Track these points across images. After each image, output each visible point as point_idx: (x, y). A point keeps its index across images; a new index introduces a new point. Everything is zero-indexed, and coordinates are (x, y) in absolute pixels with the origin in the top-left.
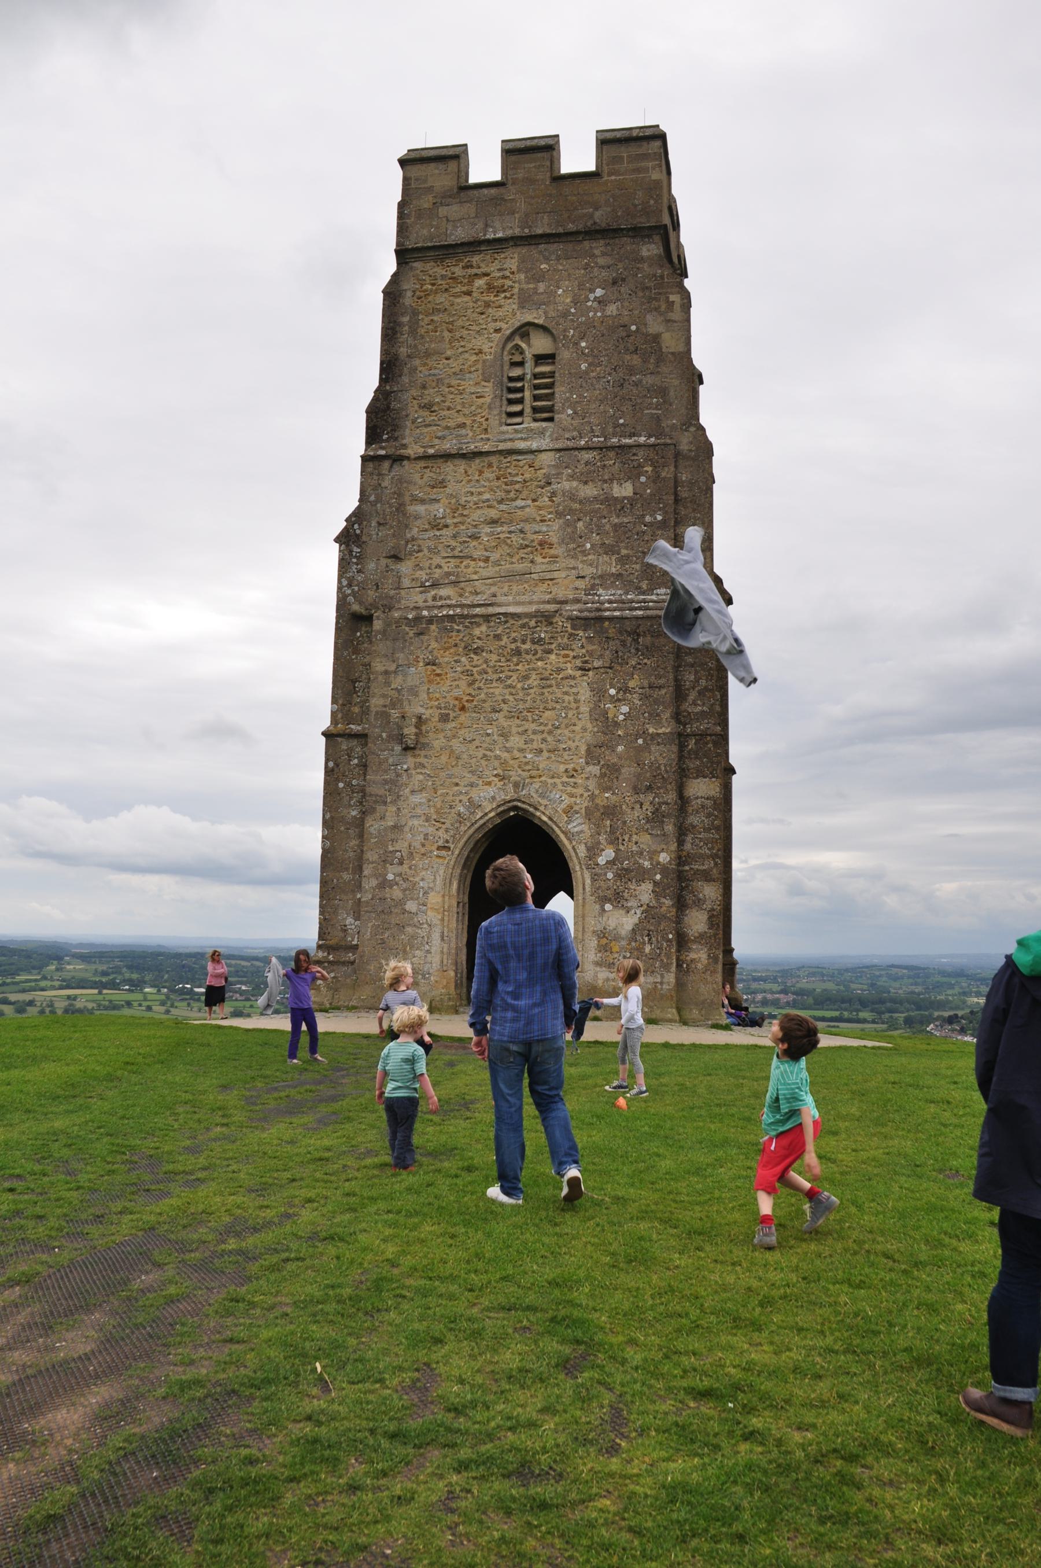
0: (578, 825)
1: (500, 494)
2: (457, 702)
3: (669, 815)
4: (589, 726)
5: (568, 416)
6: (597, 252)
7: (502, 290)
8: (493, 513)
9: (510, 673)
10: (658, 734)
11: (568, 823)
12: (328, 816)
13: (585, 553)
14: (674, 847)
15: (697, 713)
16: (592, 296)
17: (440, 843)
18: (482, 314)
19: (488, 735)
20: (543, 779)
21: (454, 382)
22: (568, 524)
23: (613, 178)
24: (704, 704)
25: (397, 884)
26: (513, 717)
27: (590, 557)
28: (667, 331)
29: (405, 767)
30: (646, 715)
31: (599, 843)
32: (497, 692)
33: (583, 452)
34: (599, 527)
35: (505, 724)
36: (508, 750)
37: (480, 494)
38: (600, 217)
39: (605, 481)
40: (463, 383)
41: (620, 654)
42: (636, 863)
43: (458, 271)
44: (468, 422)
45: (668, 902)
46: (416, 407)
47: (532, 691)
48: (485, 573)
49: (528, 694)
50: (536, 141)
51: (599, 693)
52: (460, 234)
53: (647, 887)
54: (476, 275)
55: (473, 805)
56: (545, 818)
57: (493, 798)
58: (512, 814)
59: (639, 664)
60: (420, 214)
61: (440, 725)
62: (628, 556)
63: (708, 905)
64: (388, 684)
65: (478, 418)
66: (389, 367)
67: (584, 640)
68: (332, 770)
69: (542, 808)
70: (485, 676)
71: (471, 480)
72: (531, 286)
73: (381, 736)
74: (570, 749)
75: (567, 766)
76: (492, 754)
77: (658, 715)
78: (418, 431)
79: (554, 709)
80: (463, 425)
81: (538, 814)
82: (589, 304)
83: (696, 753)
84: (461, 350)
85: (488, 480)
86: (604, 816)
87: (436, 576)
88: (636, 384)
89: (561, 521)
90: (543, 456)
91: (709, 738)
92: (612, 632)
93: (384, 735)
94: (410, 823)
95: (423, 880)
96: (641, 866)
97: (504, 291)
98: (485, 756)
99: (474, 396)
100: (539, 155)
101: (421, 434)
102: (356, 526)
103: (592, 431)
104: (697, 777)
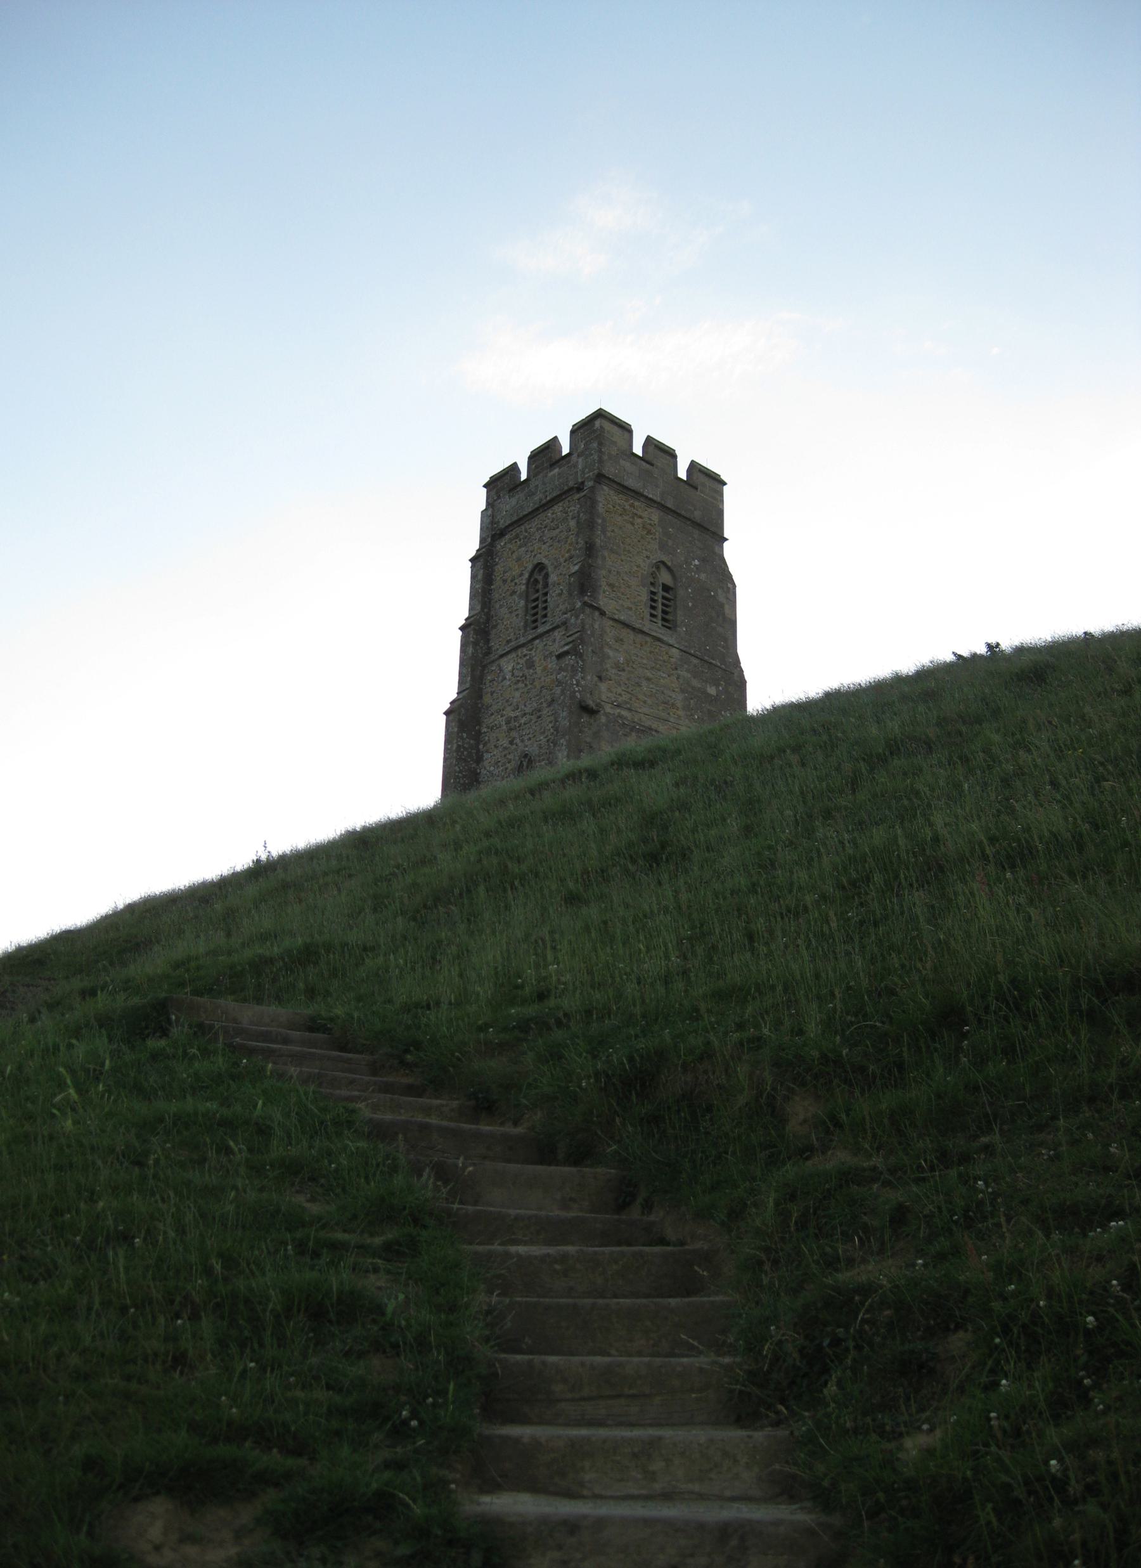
7: (649, 532)
8: (649, 674)
43: (627, 507)
52: (630, 483)
80: (630, 609)
90: (674, 650)
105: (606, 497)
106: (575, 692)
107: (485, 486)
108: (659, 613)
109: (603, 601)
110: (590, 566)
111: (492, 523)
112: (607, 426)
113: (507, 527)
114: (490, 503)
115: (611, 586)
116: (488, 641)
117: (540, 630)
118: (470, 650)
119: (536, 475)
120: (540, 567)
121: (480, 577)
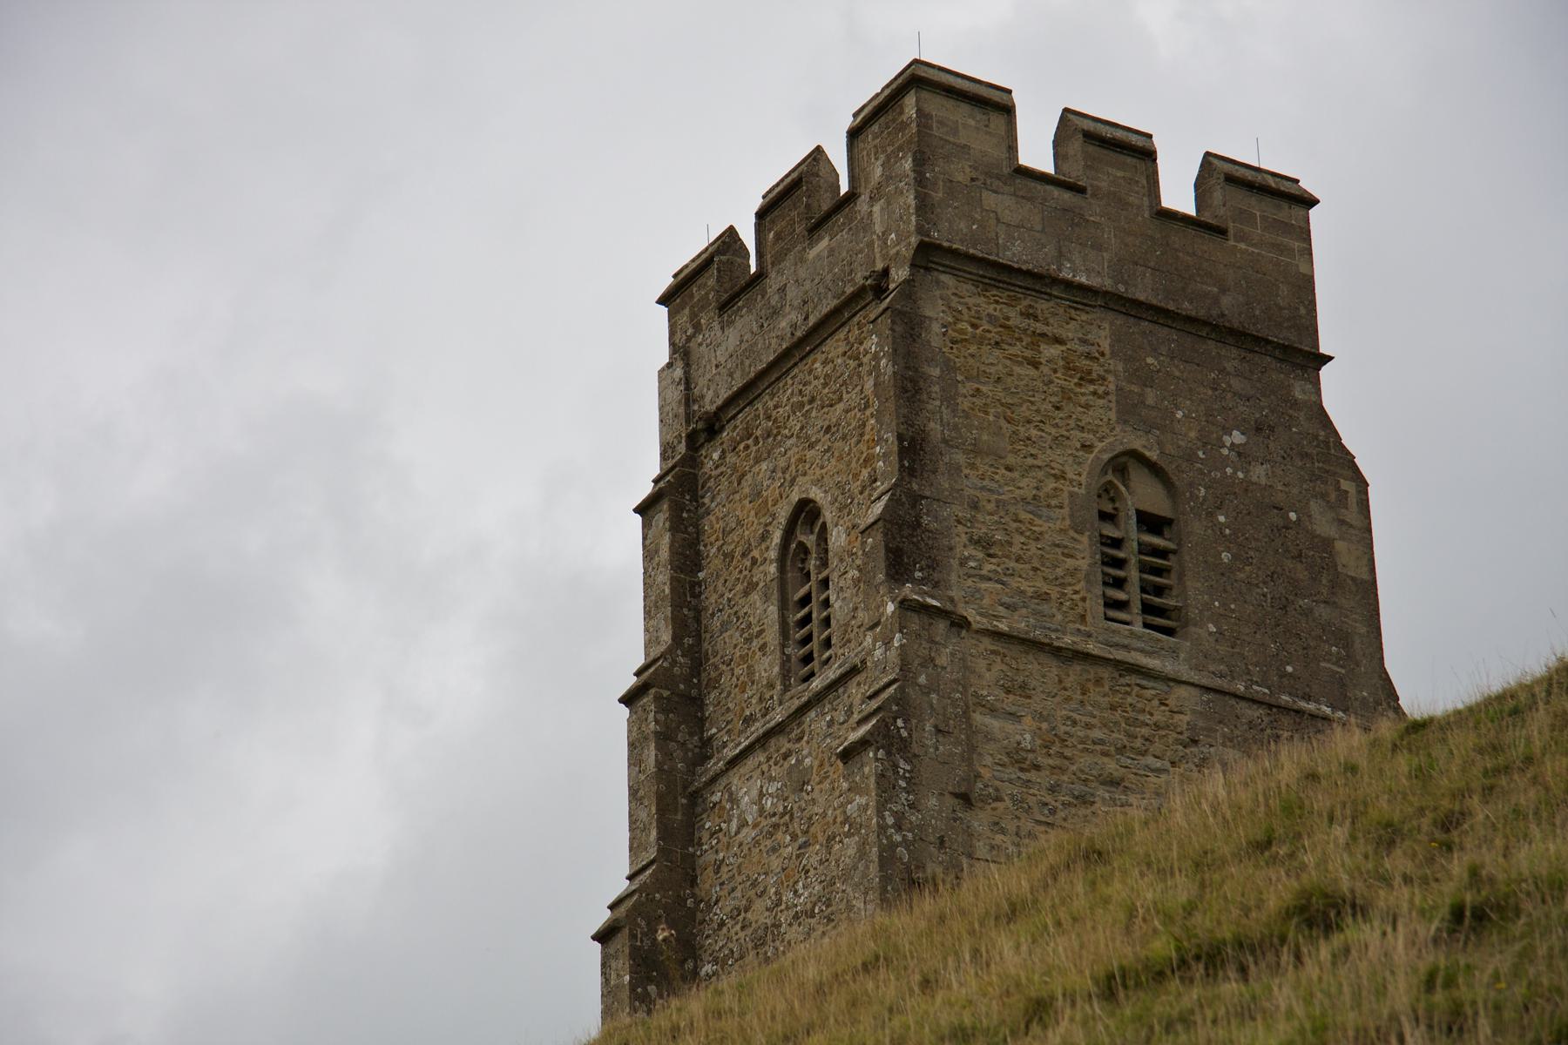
1: (1119, 737)
5: (1211, 634)
6: (1229, 366)
7: (1086, 378)
8: (1111, 766)
16: (1227, 440)
18: (1058, 408)
21: (1024, 516)
23: (1243, 246)
28: (1342, 538)
33: (1243, 704)
37: (1088, 726)
38: (1230, 306)
40: (1037, 521)
43: (1015, 320)
44: (1054, 596)
46: (964, 538)
50: (931, 71)
52: (1015, 253)
54: (1043, 335)
60: (952, 186)
65: (1068, 590)
71: (1068, 699)
72: (1135, 389)
78: (969, 582)
80: (1044, 597)
82: (1225, 452)
84: (1030, 461)
85: (1095, 705)
88: (1307, 613)
90: (1183, 692)
97: (1092, 382)
99: (1059, 550)
100: (1129, 160)
101: (978, 590)
102: (900, 723)
103: (1248, 673)
105: (947, 304)
106: (893, 846)
107: (664, 300)
108: (1132, 593)
109: (958, 591)
110: (916, 499)
111: (688, 399)
112: (939, 107)
113: (722, 409)
114: (681, 351)
115: (984, 544)
116: (700, 723)
117: (816, 684)
118: (651, 754)
119: (779, 258)
120: (806, 512)
121: (664, 554)
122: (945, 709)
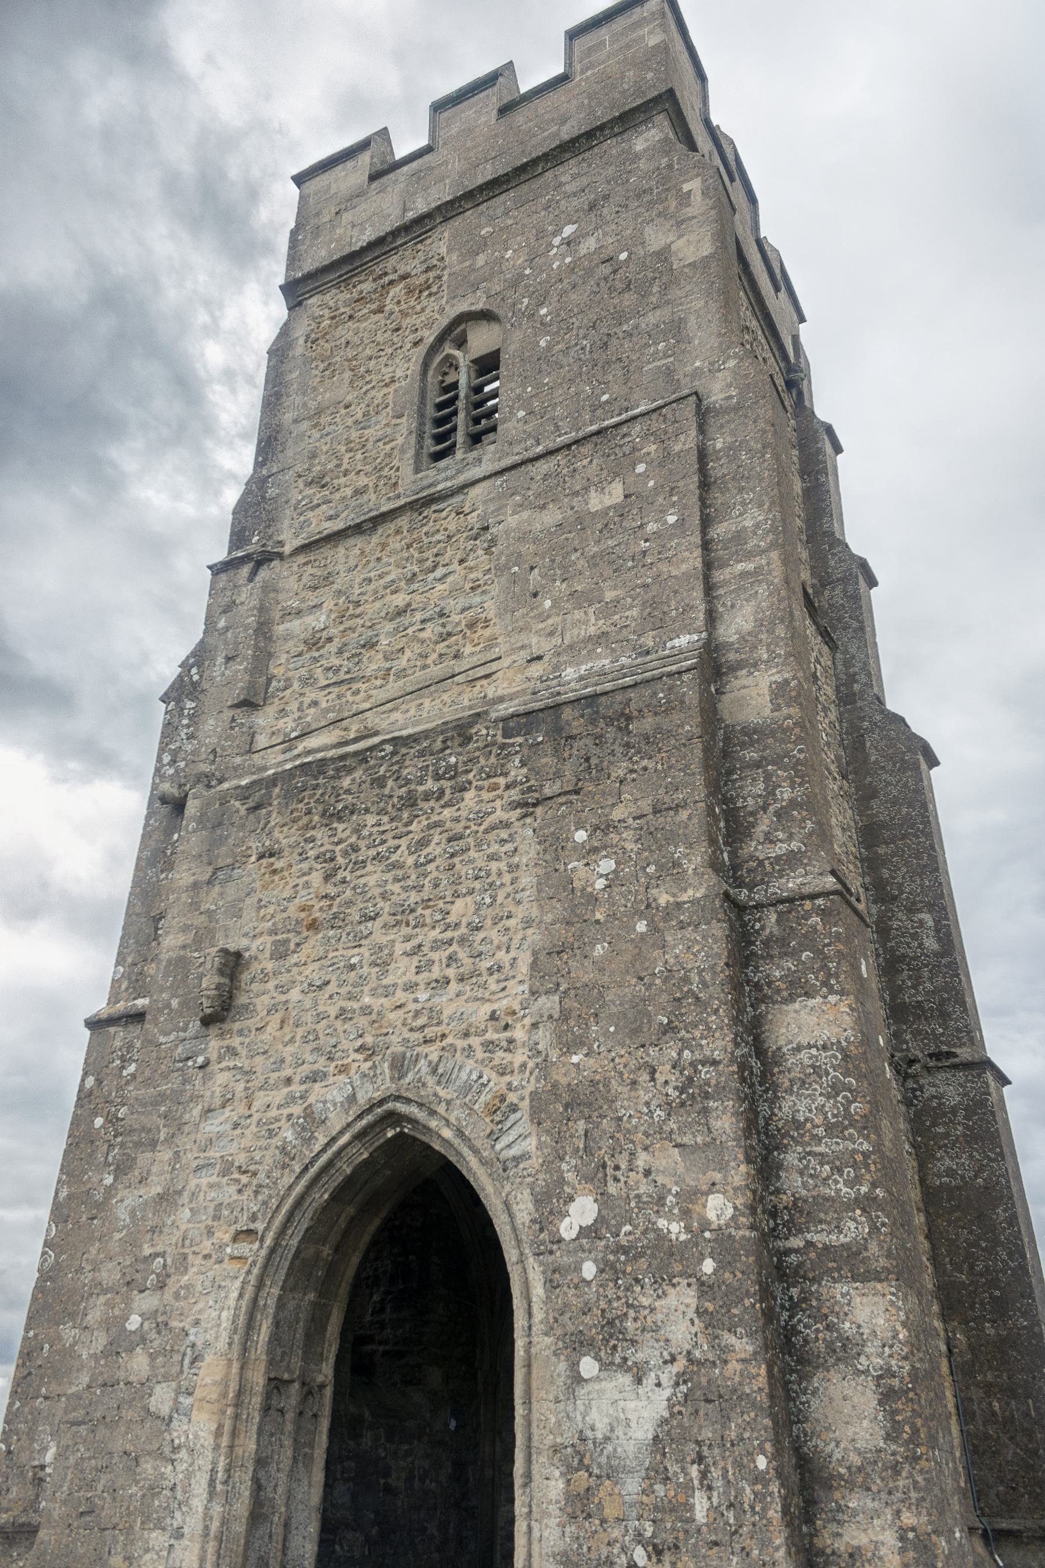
0: (524, 1140)
2: (303, 915)
3: (720, 1092)
4: (535, 913)
8: (400, 600)
9: (396, 842)
10: (679, 905)
11: (493, 1137)
12: (64, 1193)
13: (543, 617)
14: (740, 1173)
15: (778, 858)
17: (243, 1225)
19: (352, 967)
20: (449, 1040)
22: (514, 579)
24: (791, 837)
25: (143, 1340)
26: (398, 923)
27: (550, 621)
29: (200, 1060)
30: (651, 869)
31: (562, 1181)
32: (372, 880)
34: (564, 568)
35: (384, 940)
36: (388, 992)
39: (576, 494)
41: (594, 761)
42: (651, 1228)
45: (742, 1345)
47: (430, 867)
48: (382, 695)
49: (425, 875)
51: (554, 845)
53: (682, 1298)
55: (311, 1120)
56: (447, 1133)
57: (352, 1099)
58: (390, 1134)
59: (632, 771)
61: (270, 966)
62: (617, 601)
63: (872, 1359)
64: (194, 906)
66: (269, 444)
67: (526, 751)
68: (90, 1093)
69: (441, 1109)
70: (353, 857)
71: (368, 562)
73: (168, 1005)
74: (500, 968)
75: (496, 1006)
76: (356, 1005)
77: (676, 864)
78: (302, 518)
79: (471, 892)
81: (433, 1124)
83: (783, 942)
85: (394, 552)
86: (569, 1107)
87: (308, 719)
89: (503, 579)
91: (808, 905)
92: (577, 726)
93: (175, 1003)
94: (193, 1183)
95: (197, 1323)
96: (662, 1237)
98: (343, 1011)
99: (380, 444)
102: (194, 671)
104: (791, 999)
122: (236, 637)
